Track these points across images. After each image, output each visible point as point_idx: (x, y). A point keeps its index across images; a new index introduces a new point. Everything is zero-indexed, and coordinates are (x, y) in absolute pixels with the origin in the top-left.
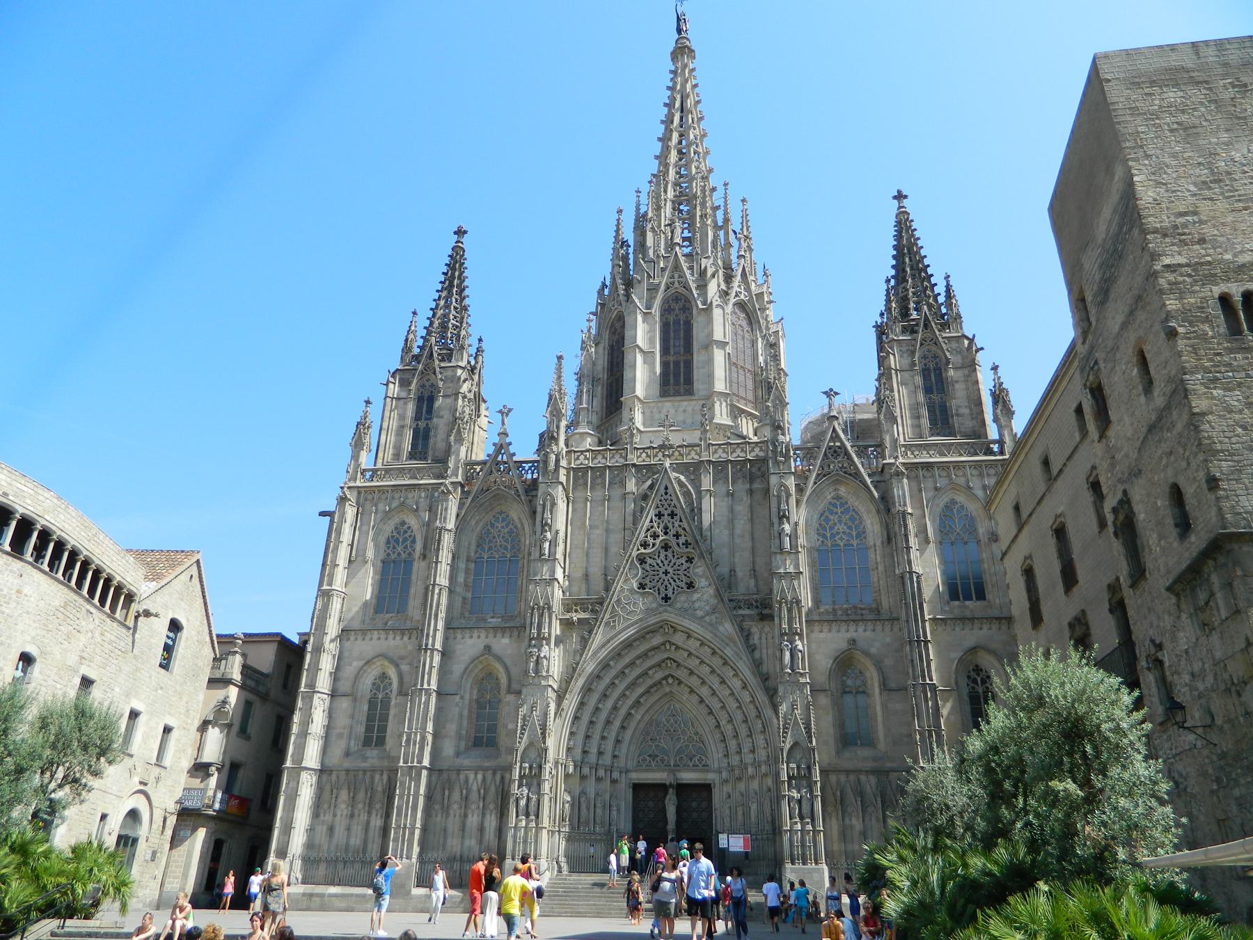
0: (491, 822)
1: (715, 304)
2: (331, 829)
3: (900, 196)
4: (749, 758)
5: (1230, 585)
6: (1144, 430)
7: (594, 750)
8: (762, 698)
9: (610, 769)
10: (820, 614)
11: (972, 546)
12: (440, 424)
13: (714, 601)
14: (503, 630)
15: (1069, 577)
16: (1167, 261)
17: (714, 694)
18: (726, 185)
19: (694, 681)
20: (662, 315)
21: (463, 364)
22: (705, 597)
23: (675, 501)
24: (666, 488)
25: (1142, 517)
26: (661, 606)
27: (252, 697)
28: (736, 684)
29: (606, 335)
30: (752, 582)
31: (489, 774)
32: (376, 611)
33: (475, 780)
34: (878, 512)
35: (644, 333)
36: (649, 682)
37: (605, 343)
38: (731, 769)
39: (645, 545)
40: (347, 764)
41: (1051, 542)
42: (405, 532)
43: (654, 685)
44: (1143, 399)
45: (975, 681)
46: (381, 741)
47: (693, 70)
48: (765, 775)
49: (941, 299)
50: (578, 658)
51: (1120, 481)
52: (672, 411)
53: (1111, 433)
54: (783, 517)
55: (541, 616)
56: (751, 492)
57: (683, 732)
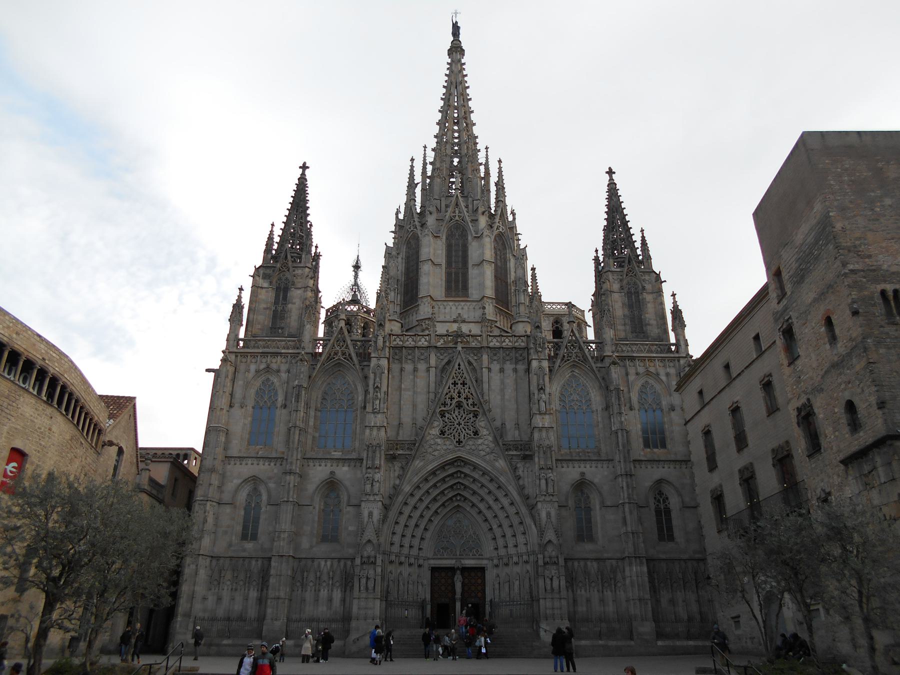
0: (337, 595)
1: (485, 234)
2: (219, 599)
3: (610, 172)
4: (512, 551)
5: (890, 464)
6: (827, 365)
7: (407, 545)
8: (524, 510)
9: (417, 558)
10: (562, 455)
11: (658, 413)
12: (294, 308)
14: (344, 460)
15: (741, 441)
16: (851, 267)
17: (490, 508)
18: (487, 148)
19: (475, 499)
20: (447, 239)
21: (310, 266)
22: (486, 442)
23: (465, 375)
24: (459, 365)
25: (821, 416)
27: (154, 501)
28: (505, 502)
29: (404, 249)
30: (517, 432)
31: (335, 562)
32: (249, 444)
33: (325, 566)
34: (600, 387)
35: (433, 249)
36: (445, 499)
37: (403, 254)
38: (500, 558)
39: (445, 404)
40: (230, 554)
41: (728, 420)
42: (270, 386)
43: (447, 500)
44: (828, 346)
45: (659, 501)
46: (254, 537)
47: (464, 64)
48: (527, 562)
49: (638, 244)
51: (805, 392)
52: (454, 308)
53: (798, 362)
54: (541, 389)
55: (374, 452)
56: (515, 370)
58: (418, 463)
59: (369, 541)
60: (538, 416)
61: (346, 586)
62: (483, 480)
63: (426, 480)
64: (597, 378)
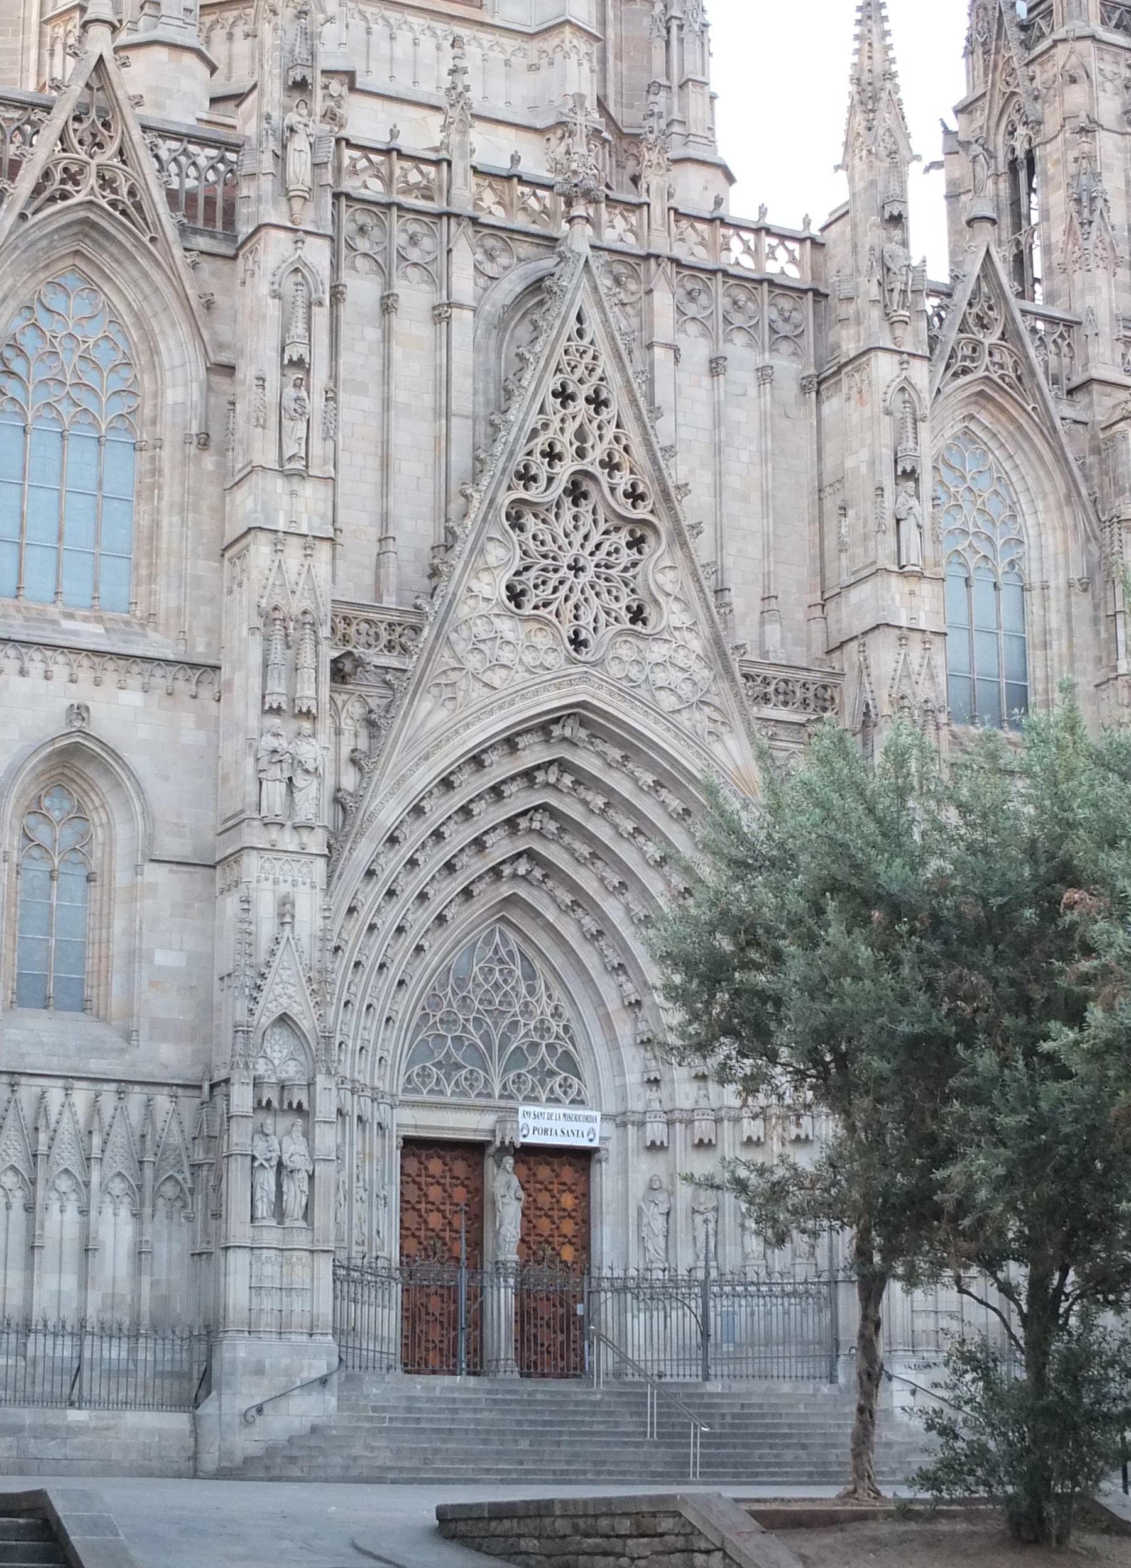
13: (702, 673)
22: (680, 660)
23: (606, 364)
24: (579, 319)
26: (572, 661)
34: (1068, 496)
39: (526, 477)
50: (349, 780)
52: (427, 44)
57: (526, 1010)
58: (426, 713)
59: (284, 1019)
60: (894, 581)
61: (157, 1193)
62: (646, 805)
63: (446, 784)
64: (1061, 458)
